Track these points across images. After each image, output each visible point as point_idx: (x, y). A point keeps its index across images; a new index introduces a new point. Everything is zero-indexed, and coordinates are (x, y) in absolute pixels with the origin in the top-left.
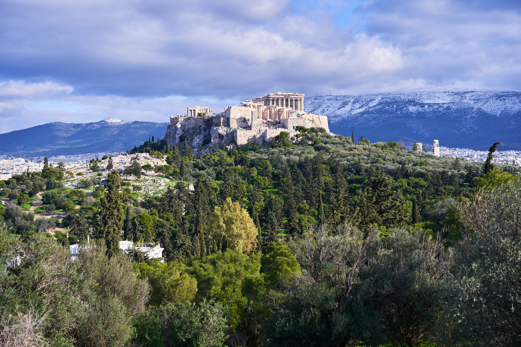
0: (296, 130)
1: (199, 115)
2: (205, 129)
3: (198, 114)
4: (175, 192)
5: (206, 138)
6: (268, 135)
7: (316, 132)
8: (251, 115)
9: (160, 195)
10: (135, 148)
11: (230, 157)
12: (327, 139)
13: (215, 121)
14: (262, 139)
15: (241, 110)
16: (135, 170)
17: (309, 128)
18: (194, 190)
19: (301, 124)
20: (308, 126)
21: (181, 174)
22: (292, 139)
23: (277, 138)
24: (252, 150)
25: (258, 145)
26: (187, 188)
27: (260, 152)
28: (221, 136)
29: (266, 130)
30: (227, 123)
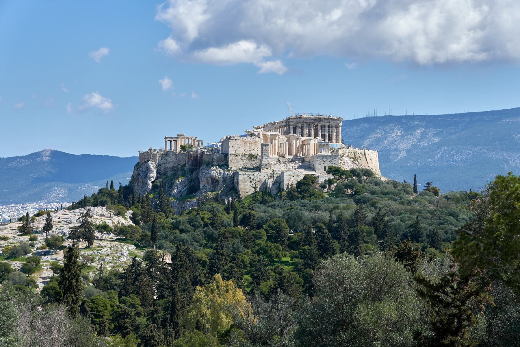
0: (328, 172)
1: (183, 148)
2: (191, 171)
3: (181, 146)
4: (144, 264)
5: (193, 183)
6: (285, 180)
7: (358, 176)
8: (260, 149)
9: (121, 270)
10: (85, 197)
11: (228, 213)
12: (375, 187)
13: (206, 159)
14: (277, 185)
15: (245, 142)
16: (85, 232)
17: (348, 169)
18: (171, 262)
19: (335, 163)
20: (347, 165)
21: (154, 238)
22: (323, 186)
23: (299, 184)
24: (261, 203)
25: (270, 194)
26: (161, 260)
27: (273, 206)
28: (214, 182)
29: (283, 173)
30: (224, 164)
